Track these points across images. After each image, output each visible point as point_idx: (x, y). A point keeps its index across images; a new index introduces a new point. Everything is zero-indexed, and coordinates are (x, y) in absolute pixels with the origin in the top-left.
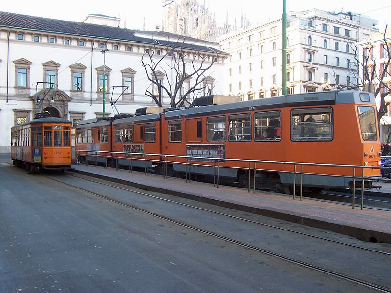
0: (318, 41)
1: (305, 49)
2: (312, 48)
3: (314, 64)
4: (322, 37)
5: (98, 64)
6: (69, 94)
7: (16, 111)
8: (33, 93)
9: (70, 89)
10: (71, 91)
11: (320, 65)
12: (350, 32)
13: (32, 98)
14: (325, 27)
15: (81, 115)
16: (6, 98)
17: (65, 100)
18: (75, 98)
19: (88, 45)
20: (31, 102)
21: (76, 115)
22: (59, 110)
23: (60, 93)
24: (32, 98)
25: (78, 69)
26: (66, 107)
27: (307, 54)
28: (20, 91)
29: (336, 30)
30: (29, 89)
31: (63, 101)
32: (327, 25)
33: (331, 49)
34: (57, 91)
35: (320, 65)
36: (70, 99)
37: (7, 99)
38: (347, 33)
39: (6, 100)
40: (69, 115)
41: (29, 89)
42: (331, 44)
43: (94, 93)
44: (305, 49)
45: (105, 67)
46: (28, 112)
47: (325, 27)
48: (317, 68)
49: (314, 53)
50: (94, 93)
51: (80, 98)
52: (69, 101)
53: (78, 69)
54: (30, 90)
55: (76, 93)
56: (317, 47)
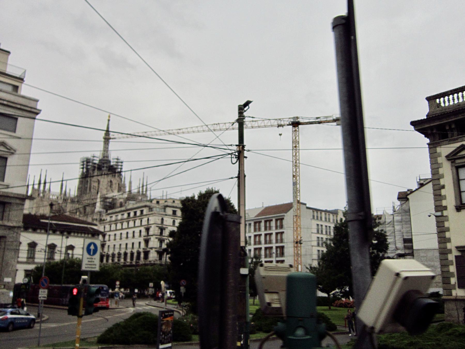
2: (164, 226)
14: (174, 212)
44: (157, 226)
47: (174, 212)
49: (165, 229)
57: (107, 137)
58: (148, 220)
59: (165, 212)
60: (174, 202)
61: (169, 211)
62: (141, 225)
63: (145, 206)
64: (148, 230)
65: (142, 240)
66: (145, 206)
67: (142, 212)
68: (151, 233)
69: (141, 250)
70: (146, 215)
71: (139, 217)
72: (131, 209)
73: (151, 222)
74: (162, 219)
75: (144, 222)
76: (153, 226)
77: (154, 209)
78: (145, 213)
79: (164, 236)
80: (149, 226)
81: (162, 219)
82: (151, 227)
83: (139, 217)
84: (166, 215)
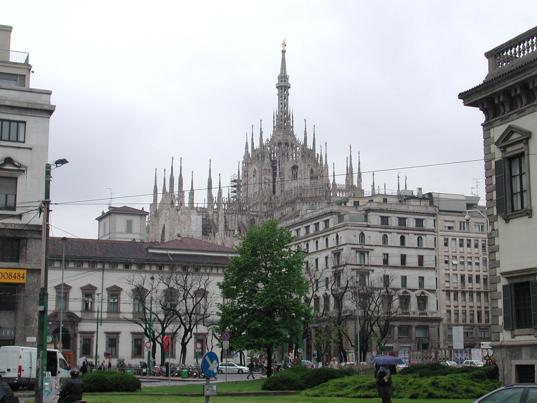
0: (373, 237)
1: (352, 249)
3: (368, 266)
4: (380, 232)
5: (108, 284)
6: (79, 315)
9: (80, 310)
10: (81, 312)
11: (376, 266)
12: (424, 221)
14: (385, 220)
15: (91, 335)
17: (73, 320)
18: (86, 318)
19: (100, 266)
21: (86, 335)
25: (89, 292)
27: (358, 255)
29: (402, 221)
31: (74, 322)
32: (405, 219)
33: (393, 245)
35: (376, 266)
36: (80, 320)
38: (419, 222)
40: (79, 335)
42: (394, 239)
43: (104, 312)
44: (352, 249)
45: (65, 285)
47: (385, 220)
48: (373, 271)
49: (368, 252)
50: (104, 312)
51: (90, 318)
52: (80, 322)
53: (89, 292)
55: (86, 314)
56: (373, 246)
57: (283, 84)
58: (337, 236)
59: (366, 220)
60: (385, 200)
61: (375, 219)
62: (327, 249)
63: (331, 213)
64: (337, 254)
65: (329, 274)
66: (331, 213)
67: (327, 222)
68: (343, 260)
69: (329, 293)
70: (334, 229)
71: (322, 232)
72: (310, 220)
73: (342, 241)
74: (362, 235)
75: (332, 243)
76: (345, 248)
77: (346, 217)
78: (331, 225)
79: (368, 266)
80: (339, 248)
81: (362, 235)
82: (342, 250)
83: (322, 232)
84: (369, 226)
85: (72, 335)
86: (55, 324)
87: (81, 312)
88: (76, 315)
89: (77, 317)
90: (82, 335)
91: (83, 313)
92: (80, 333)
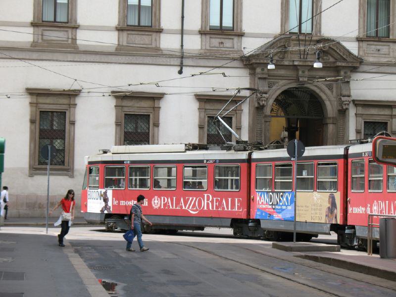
6: (353, 48)
7: (204, 100)
8: (250, 46)
9: (355, 34)
10: (359, 40)
13: (250, 63)
15: (387, 112)
16: (178, 62)
17: (341, 63)
18: (371, 59)
20: (245, 73)
22: (322, 94)
23: (330, 50)
24: (250, 63)
26: (343, 86)
28: (215, 42)
30: (241, 35)
34: (318, 41)
36: (355, 65)
37: (181, 66)
39: (178, 69)
41: (241, 35)
46: (236, 100)
51: (384, 60)
52: (354, 69)
54: (244, 39)
55: (374, 47)
85: (331, 109)
86: (282, 77)
87: (359, 40)
88: (344, 48)
89: (350, 54)
90: (361, 110)
91: (364, 45)
92: (357, 103)
